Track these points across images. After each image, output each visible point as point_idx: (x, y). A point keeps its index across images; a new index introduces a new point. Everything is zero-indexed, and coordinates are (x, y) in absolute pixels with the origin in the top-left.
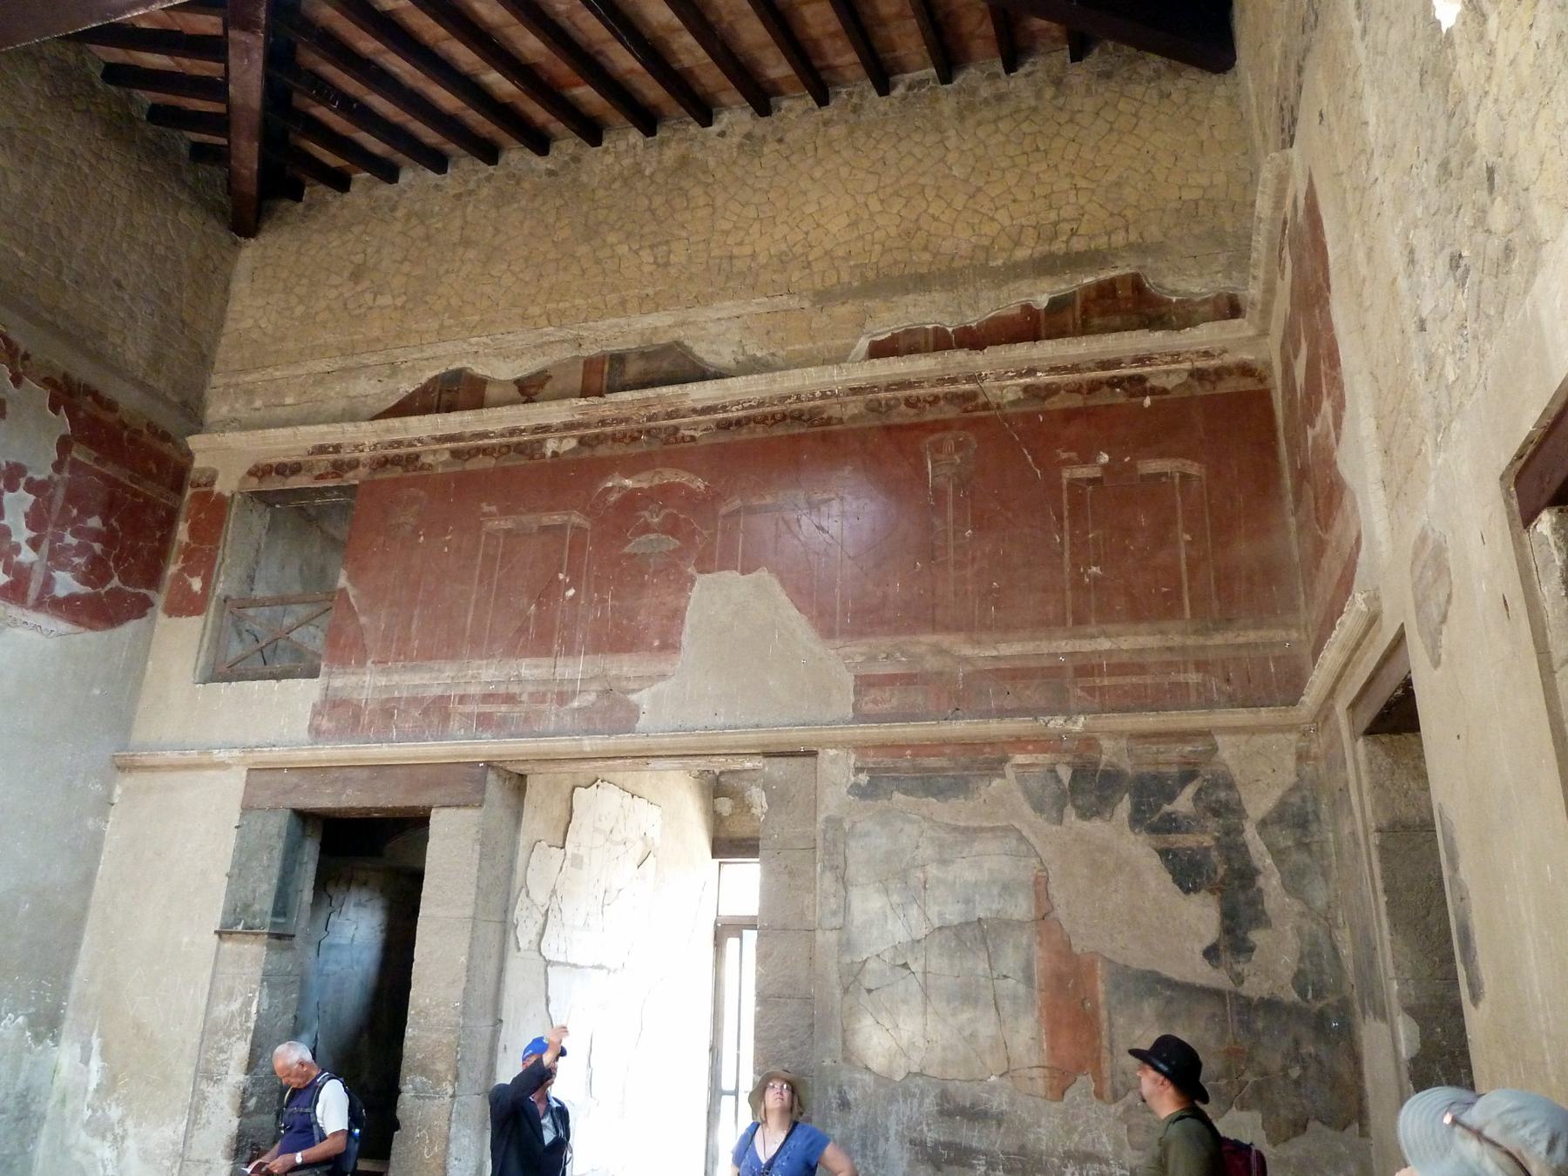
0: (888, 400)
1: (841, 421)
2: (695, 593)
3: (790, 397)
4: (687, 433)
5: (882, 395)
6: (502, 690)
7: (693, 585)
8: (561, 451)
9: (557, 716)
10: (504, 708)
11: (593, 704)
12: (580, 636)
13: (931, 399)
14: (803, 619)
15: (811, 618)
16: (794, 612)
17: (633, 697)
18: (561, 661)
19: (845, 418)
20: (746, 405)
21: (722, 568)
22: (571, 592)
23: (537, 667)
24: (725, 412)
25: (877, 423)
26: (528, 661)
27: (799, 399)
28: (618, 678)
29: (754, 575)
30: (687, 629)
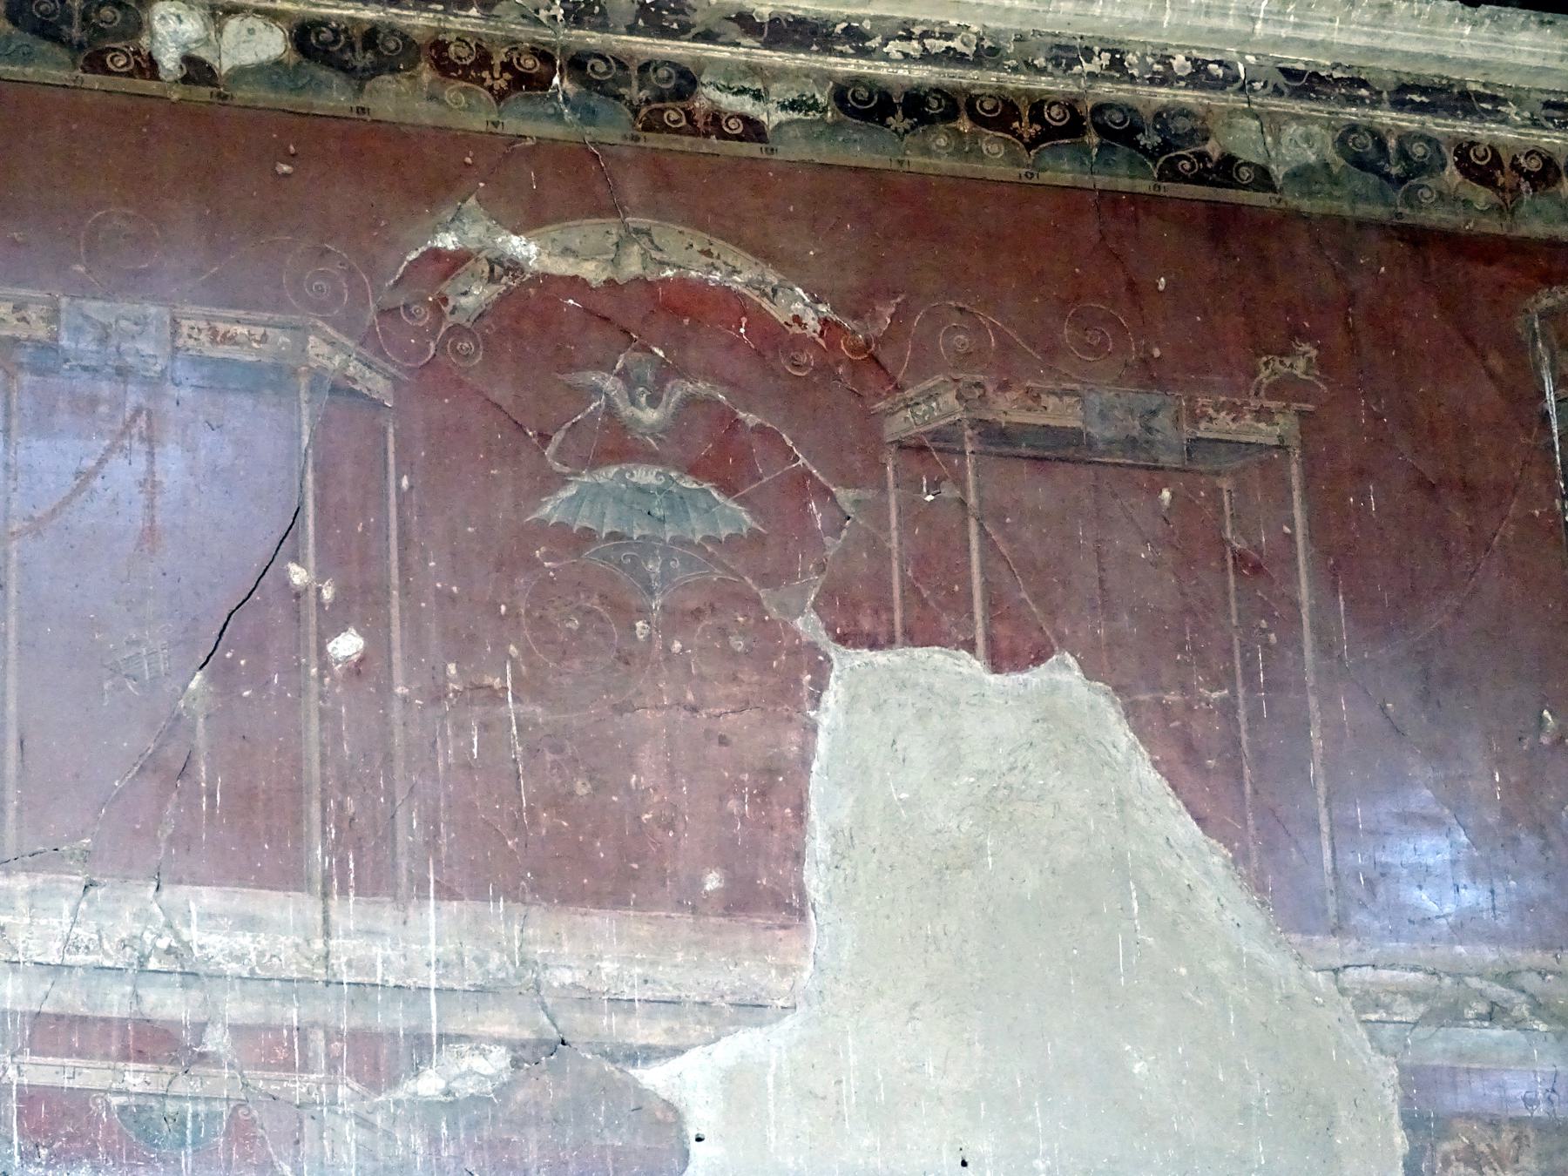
0: (1405, 138)
1: (1263, 179)
2: (831, 711)
3: (1088, 54)
4: (729, 102)
5: (1386, 117)
6: (115, 1002)
7: (820, 685)
8: (225, 65)
9: (364, 1123)
10: (136, 1078)
11: (504, 1090)
12: (409, 827)
13: (1534, 165)
14: (1218, 858)
15: (1240, 858)
16: (1185, 828)
17: (652, 1077)
18: (348, 912)
19: (1278, 172)
20: (938, 45)
21: (914, 637)
22: (347, 645)
23: (250, 923)
24: (864, 53)
25: (1379, 211)
26: (209, 897)
27: (1117, 63)
28: (586, 1000)
29: (1036, 677)
30: (818, 844)
